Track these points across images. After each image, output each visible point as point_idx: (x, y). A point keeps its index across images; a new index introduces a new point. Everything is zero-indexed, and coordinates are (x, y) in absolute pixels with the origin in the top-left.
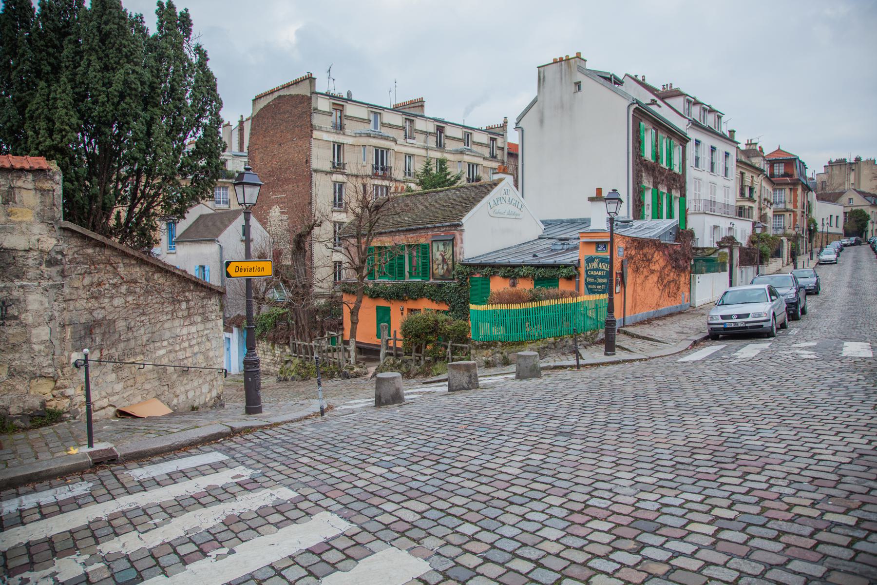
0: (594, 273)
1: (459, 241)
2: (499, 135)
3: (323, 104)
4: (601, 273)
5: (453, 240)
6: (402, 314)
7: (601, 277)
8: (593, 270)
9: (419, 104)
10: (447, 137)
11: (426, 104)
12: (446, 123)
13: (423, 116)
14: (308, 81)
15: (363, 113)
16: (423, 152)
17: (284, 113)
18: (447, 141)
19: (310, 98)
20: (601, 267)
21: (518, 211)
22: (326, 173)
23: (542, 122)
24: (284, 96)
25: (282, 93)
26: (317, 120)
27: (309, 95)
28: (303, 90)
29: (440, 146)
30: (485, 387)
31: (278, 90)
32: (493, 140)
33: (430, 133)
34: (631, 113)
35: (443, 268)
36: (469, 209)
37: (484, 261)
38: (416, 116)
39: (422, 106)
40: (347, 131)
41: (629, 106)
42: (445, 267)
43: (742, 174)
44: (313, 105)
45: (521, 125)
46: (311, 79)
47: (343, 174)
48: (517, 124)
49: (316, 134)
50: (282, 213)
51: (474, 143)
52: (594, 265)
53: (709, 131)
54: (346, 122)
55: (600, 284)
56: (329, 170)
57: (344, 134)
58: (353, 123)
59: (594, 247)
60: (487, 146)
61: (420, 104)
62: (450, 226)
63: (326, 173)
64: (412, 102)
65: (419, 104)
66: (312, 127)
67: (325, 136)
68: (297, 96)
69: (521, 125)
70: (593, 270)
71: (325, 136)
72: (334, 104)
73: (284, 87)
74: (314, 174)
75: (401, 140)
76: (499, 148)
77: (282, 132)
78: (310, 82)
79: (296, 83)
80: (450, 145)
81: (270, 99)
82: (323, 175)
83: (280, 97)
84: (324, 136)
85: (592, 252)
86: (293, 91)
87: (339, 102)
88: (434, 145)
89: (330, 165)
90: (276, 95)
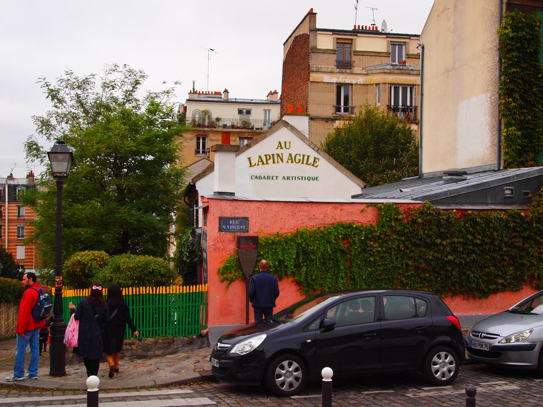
3: (325, 42)
15: (380, 45)
22: (327, 120)
26: (315, 61)
28: (305, 30)
44: (311, 44)
49: (314, 77)
54: (354, 58)
57: (351, 73)
63: (327, 120)
66: (308, 70)
67: (326, 78)
68: (303, 34)
71: (326, 78)
72: (337, 39)
83: (296, 38)
89: (333, 110)
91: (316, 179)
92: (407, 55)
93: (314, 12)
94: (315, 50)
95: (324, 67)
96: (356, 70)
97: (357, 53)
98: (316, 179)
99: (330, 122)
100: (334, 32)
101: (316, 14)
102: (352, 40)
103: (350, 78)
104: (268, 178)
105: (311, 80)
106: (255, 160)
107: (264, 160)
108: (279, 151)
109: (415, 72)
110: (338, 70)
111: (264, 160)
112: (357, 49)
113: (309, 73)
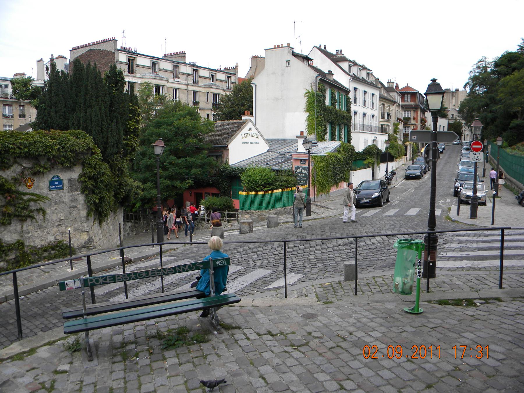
0: (300, 175)
1: (226, 155)
2: (232, 74)
4: (303, 175)
6: (191, 195)
7: (303, 177)
8: (299, 173)
9: (183, 55)
10: (200, 77)
11: (186, 56)
12: (200, 67)
13: (185, 63)
16: (185, 87)
18: (200, 80)
19: (113, 54)
20: (303, 171)
24: (95, 50)
25: (93, 48)
27: (113, 51)
29: (195, 82)
30: (255, 231)
31: (89, 45)
32: (229, 77)
33: (189, 74)
38: (181, 63)
39: (184, 57)
42: (217, 170)
43: (383, 105)
51: (217, 80)
52: (300, 170)
53: (363, 82)
54: (135, 68)
55: (303, 180)
58: (141, 69)
59: (299, 162)
60: (225, 82)
61: (183, 55)
64: (177, 54)
65: (183, 55)
70: (299, 173)
75: (171, 80)
76: (233, 83)
78: (114, 43)
79: (103, 42)
80: (202, 82)
83: (91, 50)
85: (298, 164)
88: (191, 82)
90: (88, 49)
91: (258, 143)
94: (119, 62)
96: (138, 75)
97: (138, 66)
98: (258, 143)
104: (247, 143)
106: (243, 136)
107: (247, 135)
108: (249, 132)
110: (129, 74)
111: (247, 135)
112: (138, 63)
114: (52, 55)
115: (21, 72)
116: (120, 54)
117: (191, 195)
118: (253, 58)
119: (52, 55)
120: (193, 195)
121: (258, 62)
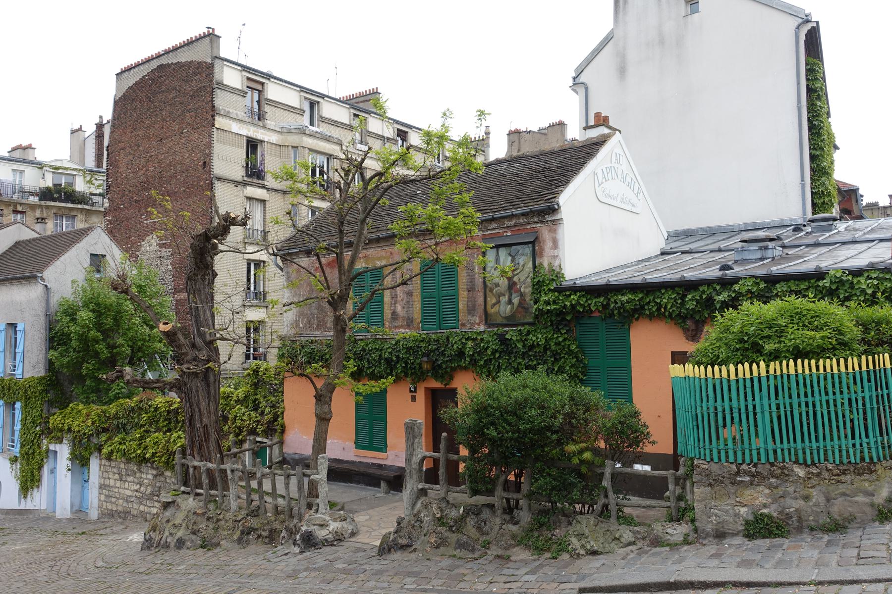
1: (549, 244)
3: (231, 78)
5: (533, 243)
6: (414, 399)
12: (410, 127)
14: (208, 38)
15: (292, 98)
17: (168, 91)
19: (211, 67)
21: (634, 200)
22: (236, 183)
23: (622, 71)
24: (169, 65)
25: (164, 61)
26: (222, 100)
27: (209, 61)
31: (159, 56)
33: (388, 139)
34: (803, 38)
35: (510, 302)
36: (567, 183)
37: (614, 278)
40: (270, 123)
41: (798, 27)
42: (516, 300)
44: (217, 77)
45: (582, 79)
46: (211, 37)
47: (263, 187)
48: (574, 79)
49: (220, 122)
50: (161, 246)
54: (267, 108)
56: (239, 179)
57: (264, 127)
58: (279, 112)
62: (532, 213)
63: (236, 183)
66: (213, 111)
67: (235, 127)
68: (190, 64)
69: (582, 79)
71: (235, 127)
72: (248, 79)
73: (167, 52)
74: (218, 185)
77: (164, 120)
78: (211, 41)
79: (189, 43)
81: (144, 71)
82: (232, 186)
83: (161, 67)
84: (233, 124)
86: (183, 57)
87: (257, 81)
90: (155, 64)
92: (321, 117)
93: (216, 33)
95: (234, 112)
97: (270, 102)
99: (240, 187)
100: (245, 68)
101: (220, 37)
102: (263, 84)
103: (262, 133)
105: (217, 126)
109: (336, 140)
112: (270, 97)
113: (213, 116)
114: (101, 117)
115: (24, 144)
116: (225, 68)
117: (414, 399)
118: (511, 133)
119: (101, 117)
120: (421, 395)
121: (522, 140)
